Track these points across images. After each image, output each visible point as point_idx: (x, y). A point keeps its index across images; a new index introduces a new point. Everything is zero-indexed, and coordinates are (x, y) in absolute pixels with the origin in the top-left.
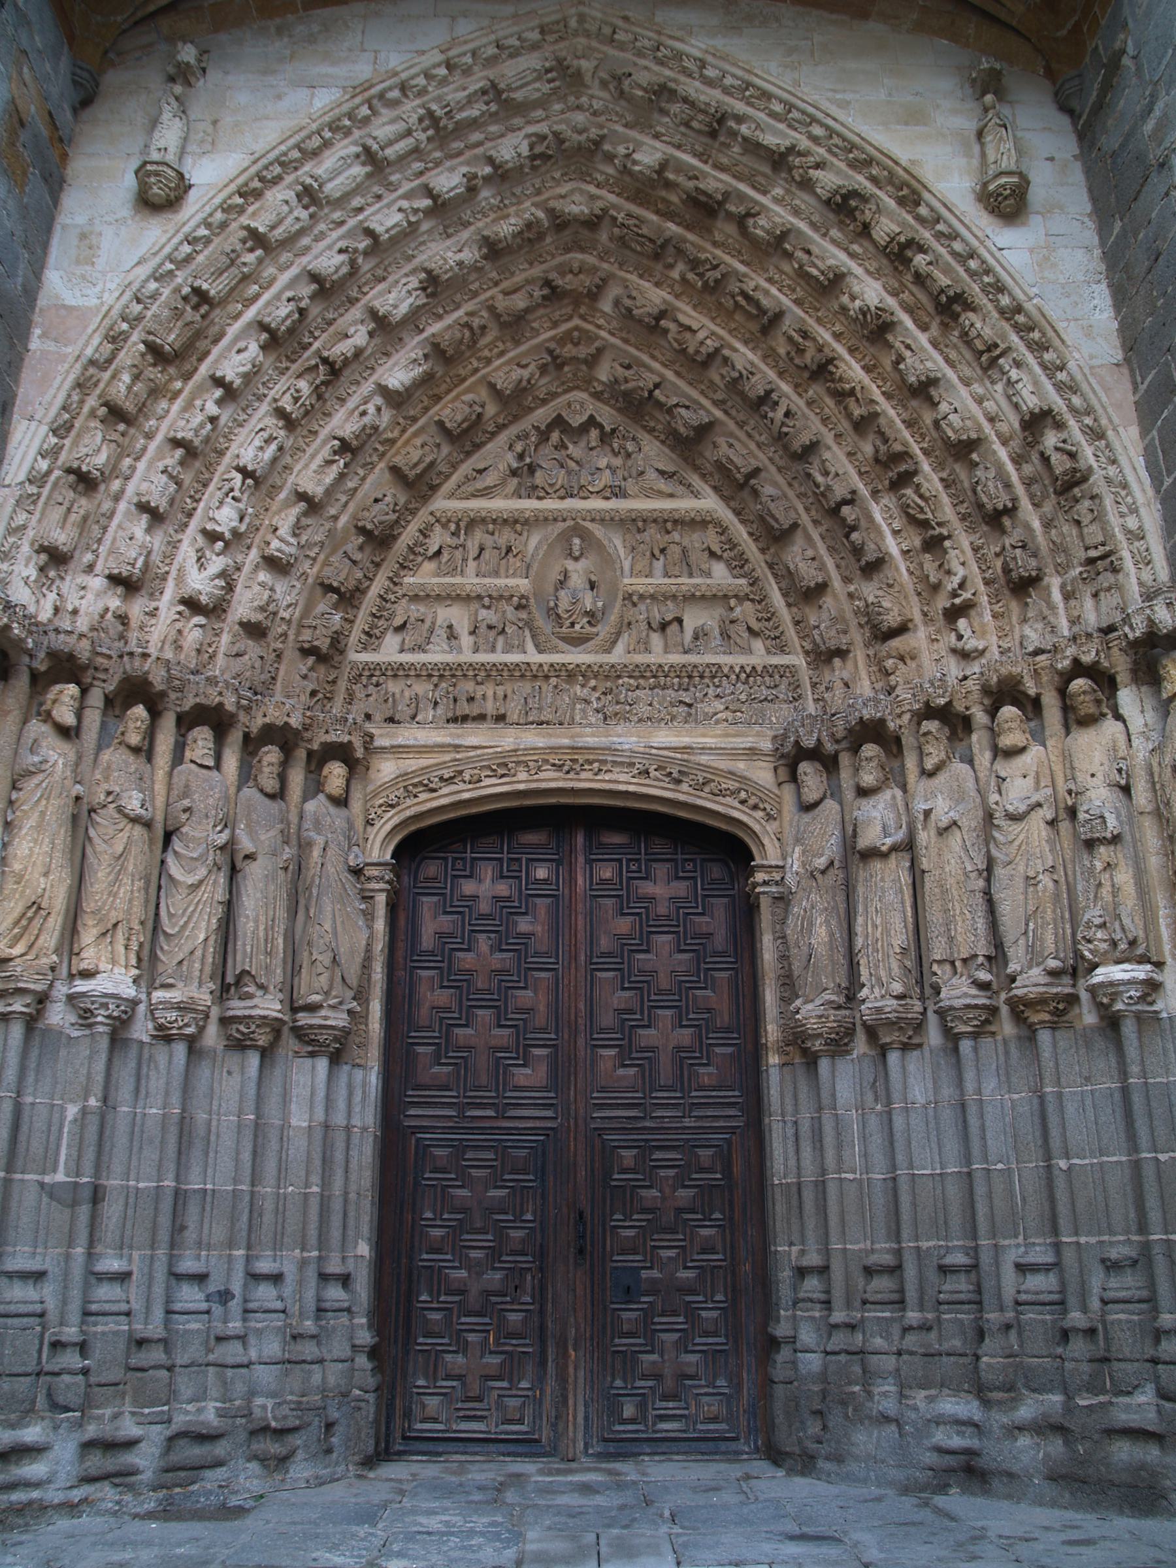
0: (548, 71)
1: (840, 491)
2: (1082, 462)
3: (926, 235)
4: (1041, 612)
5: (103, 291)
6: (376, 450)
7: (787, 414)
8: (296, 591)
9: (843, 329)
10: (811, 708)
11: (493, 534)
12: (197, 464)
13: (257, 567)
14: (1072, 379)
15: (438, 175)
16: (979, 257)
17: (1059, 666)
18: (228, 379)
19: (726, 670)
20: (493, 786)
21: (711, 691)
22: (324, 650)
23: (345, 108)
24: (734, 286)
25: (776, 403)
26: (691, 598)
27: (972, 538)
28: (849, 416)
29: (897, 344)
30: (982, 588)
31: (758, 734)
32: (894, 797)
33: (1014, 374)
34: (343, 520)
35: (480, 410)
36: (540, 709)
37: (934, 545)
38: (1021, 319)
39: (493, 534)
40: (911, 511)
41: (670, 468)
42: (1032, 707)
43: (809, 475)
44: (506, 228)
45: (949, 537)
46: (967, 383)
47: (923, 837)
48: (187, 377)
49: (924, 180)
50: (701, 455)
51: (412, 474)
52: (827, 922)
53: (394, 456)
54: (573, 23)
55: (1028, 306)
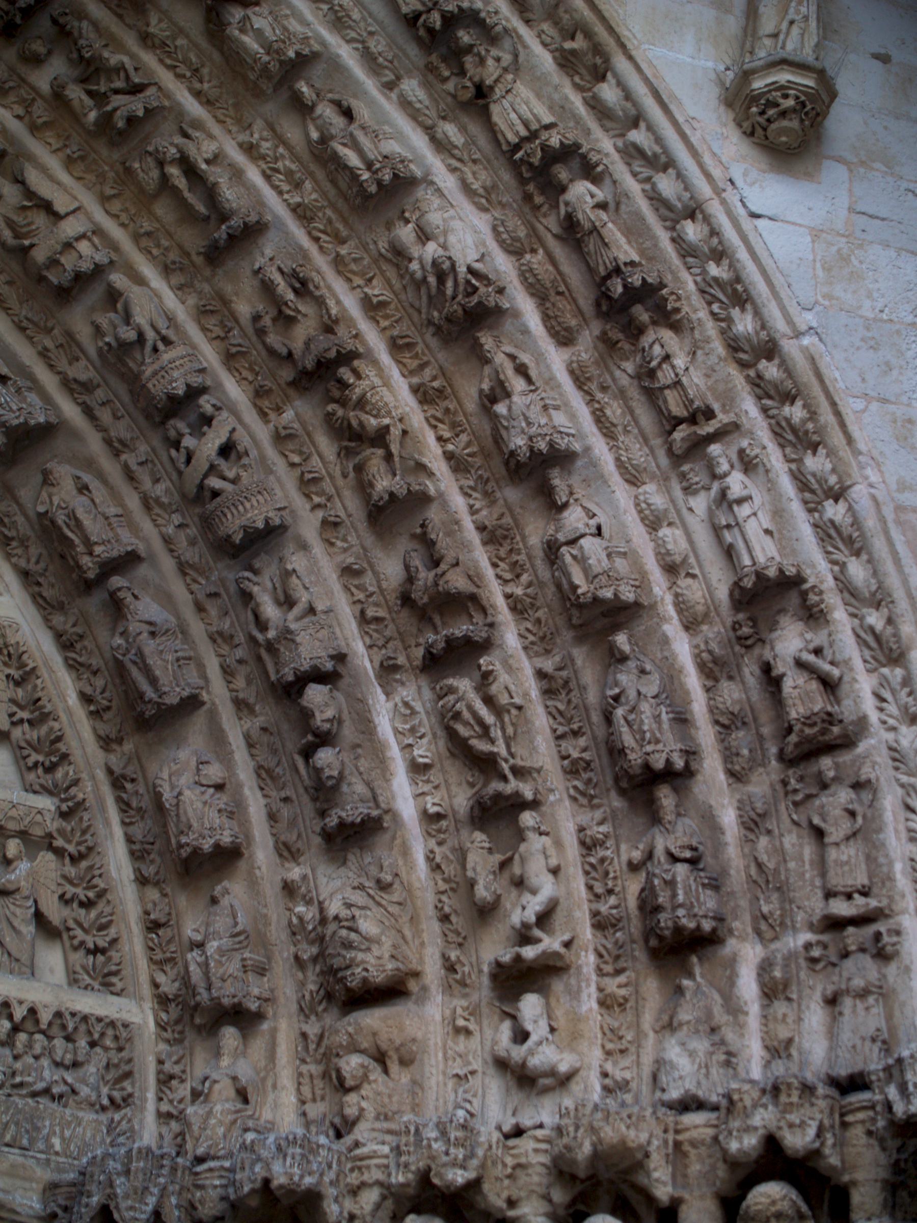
2: (847, 703)
4: (709, 1015)
7: (227, 450)
9: (387, 296)
14: (856, 523)
16: (707, 219)
17: (734, 1146)
25: (208, 420)
27: (585, 818)
28: (364, 487)
29: (500, 359)
30: (587, 933)
33: (737, 483)
38: (771, 370)
40: (463, 731)
43: (247, 597)
45: (534, 805)
46: (633, 478)
49: (624, 32)
55: (789, 347)
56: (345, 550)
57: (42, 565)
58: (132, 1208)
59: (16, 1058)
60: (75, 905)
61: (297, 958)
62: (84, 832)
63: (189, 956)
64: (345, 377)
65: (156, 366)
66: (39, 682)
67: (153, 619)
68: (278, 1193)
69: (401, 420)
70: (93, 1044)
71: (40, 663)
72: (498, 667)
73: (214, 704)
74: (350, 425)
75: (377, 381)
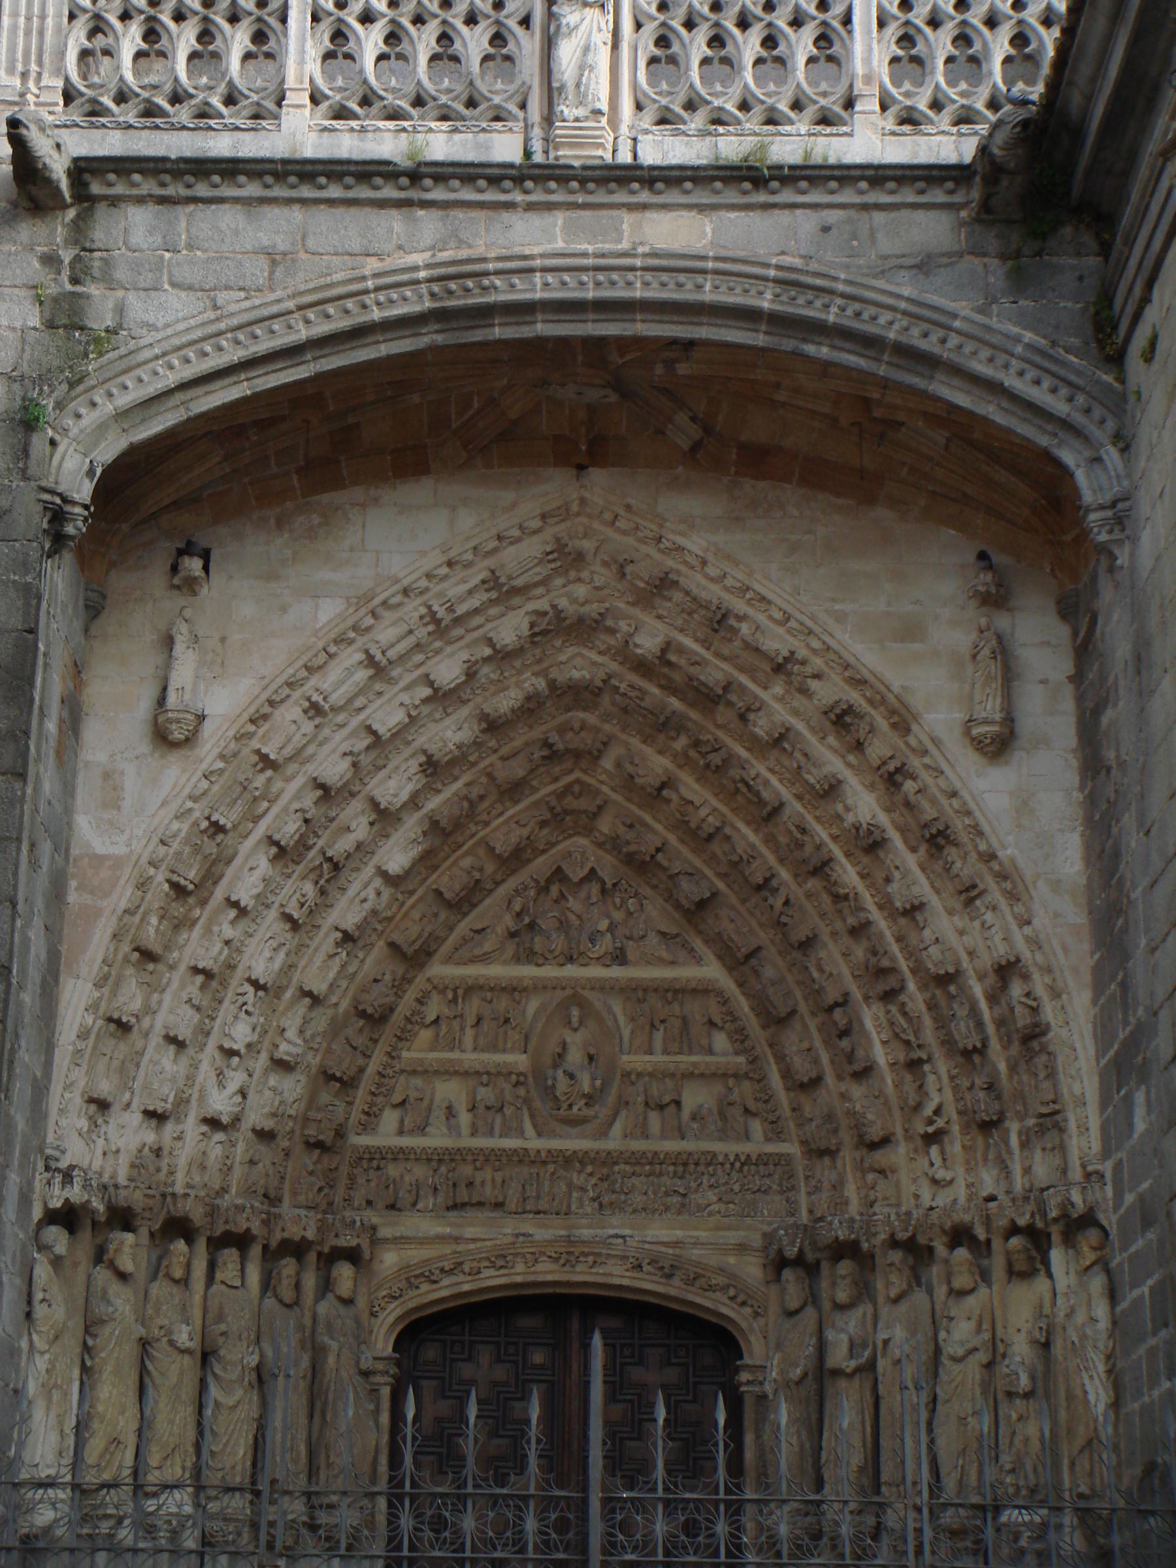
0: (548, 554)
1: (832, 995)
3: (915, 763)
5: (130, 839)
7: (787, 903)
8: (301, 1084)
11: (490, 1002)
12: (214, 984)
13: (266, 1072)
15: (438, 663)
18: (243, 904)
20: (492, 1278)
21: (705, 1178)
22: (329, 1143)
23: (350, 622)
24: (735, 773)
30: (955, 1116)
32: (865, 1315)
33: (989, 917)
34: (345, 1004)
36: (538, 1197)
37: (914, 1065)
39: (490, 1002)
42: (982, 1249)
43: (807, 968)
44: (506, 702)
45: (929, 1060)
46: (951, 912)
47: (881, 1364)
48: (203, 903)
51: (410, 951)
52: (798, 1431)
54: (575, 508)
72: (907, 1000)
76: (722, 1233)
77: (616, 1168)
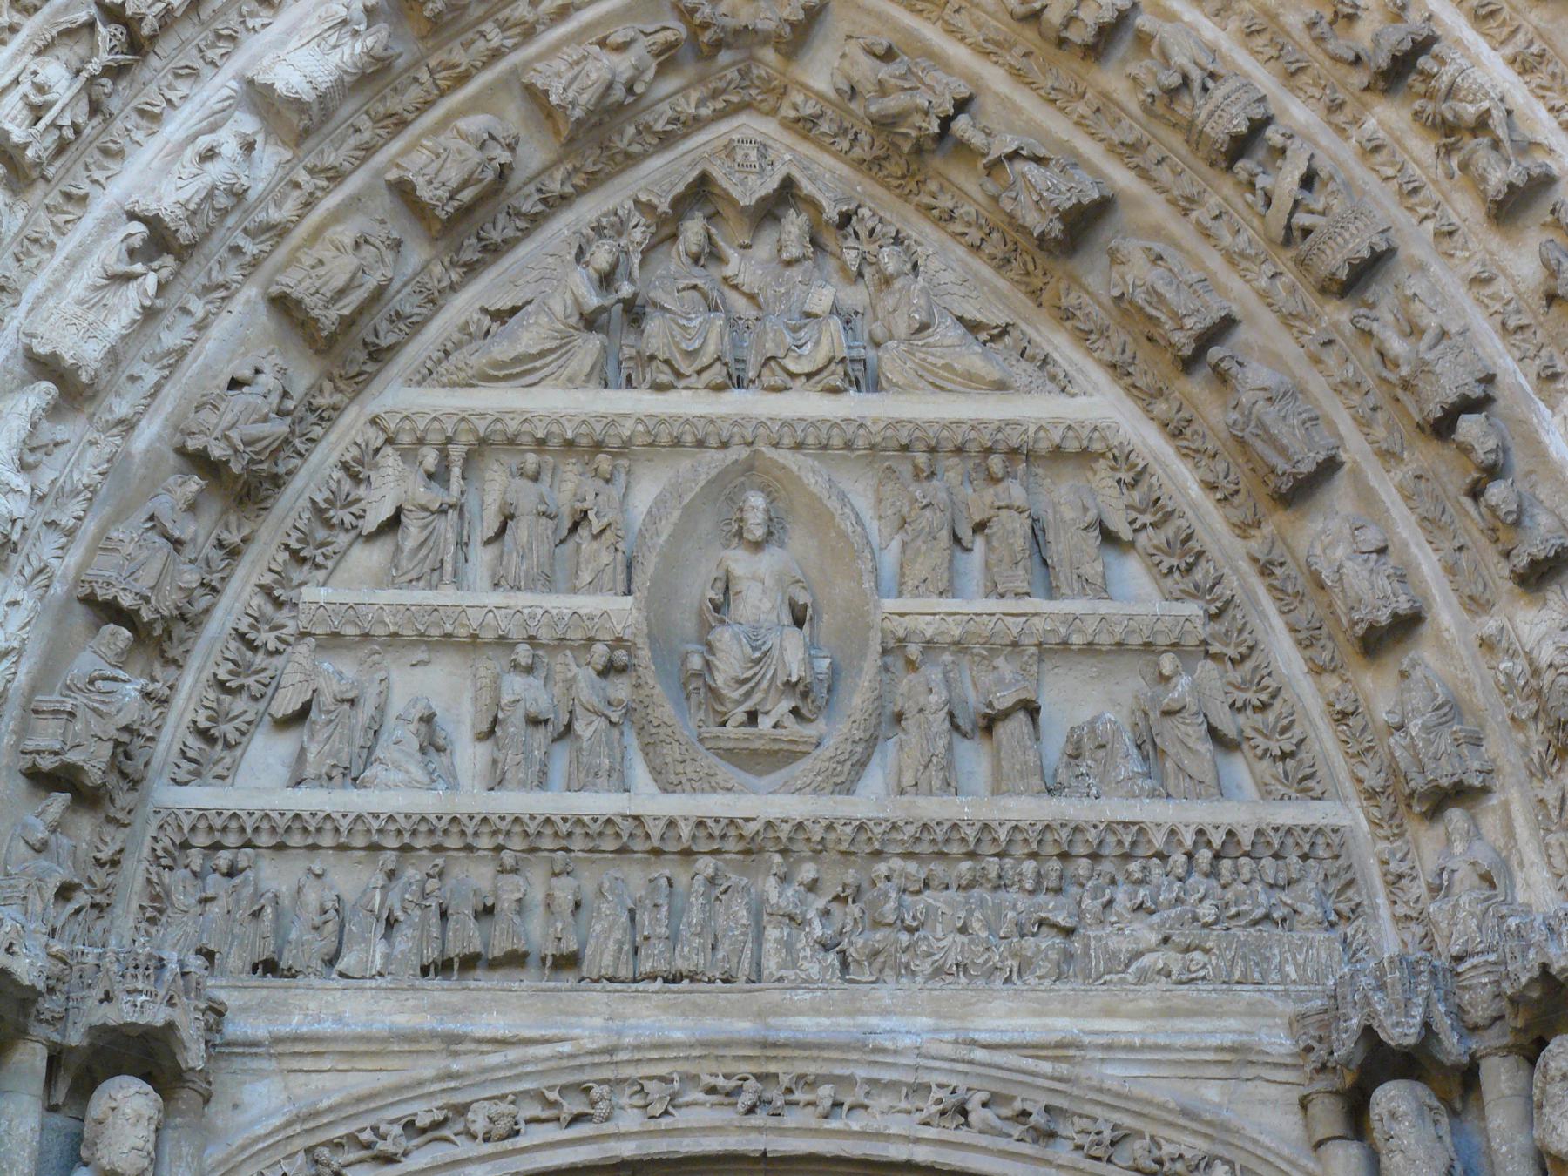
1: (1451, 382)
6: (236, 250)
7: (1308, 181)
8: (18, 617)
10: (1389, 941)
11: (535, 478)
19: (1159, 841)
21: (1121, 894)
22: (94, 776)
26: (1056, 650)
28: (1478, 182)
31: (1252, 1011)
35: (504, 157)
36: (673, 939)
39: (535, 478)
41: (997, 317)
50: (1074, 280)
53: (282, 268)
56: (1468, 259)
57: (1129, 353)
58: (1398, 1024)
59: (1224, 887)
60: (1249, 711)
61: (1513, 718)
62: (1240, 631)
63: (1391, 741)
64: (1427, 67)
65: (1210, 107)
66: (1154, 480)
67: (1267, 384)
68: (1562, 978)
69: (1502, 100)
70: (1304, 857)
71: (1151, 461)
73: (1355, 462)
74: (1444, 121)
75: (1464, 63)
76: (1181, 1024)
77: (882, 868)
